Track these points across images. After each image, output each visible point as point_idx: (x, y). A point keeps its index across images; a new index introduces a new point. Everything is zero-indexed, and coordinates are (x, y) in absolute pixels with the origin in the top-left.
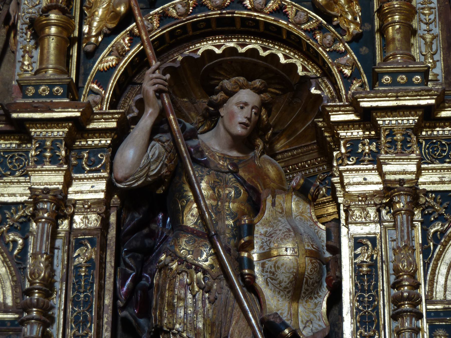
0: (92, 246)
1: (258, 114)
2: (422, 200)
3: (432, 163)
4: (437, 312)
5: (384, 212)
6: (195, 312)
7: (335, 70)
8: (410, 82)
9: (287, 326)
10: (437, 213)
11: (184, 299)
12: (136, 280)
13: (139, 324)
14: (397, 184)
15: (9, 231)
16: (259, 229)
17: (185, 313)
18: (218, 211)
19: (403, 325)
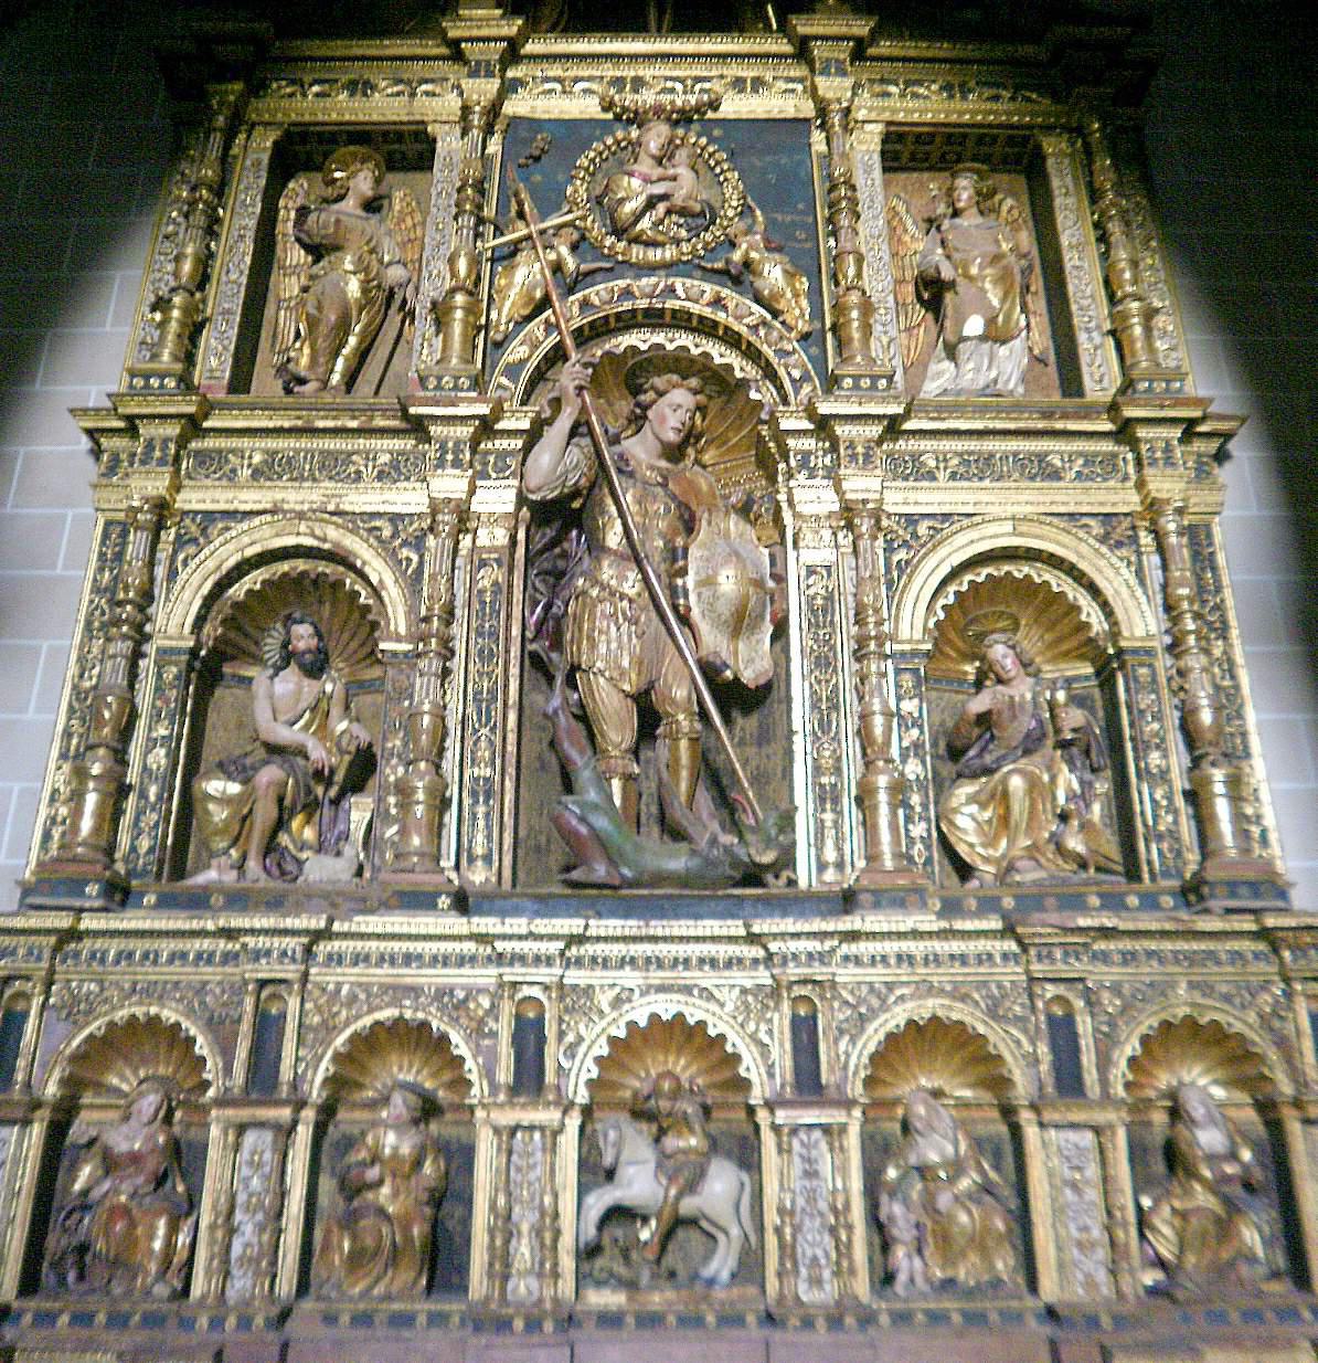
0: (500, 566)
1: (692, 418)
2: (885, 523)
4: (903, 654)
5: (840, 535)
6: (620, 647)
7: (782, 372)
8: (873, 387)
9: (728, 667)
11: (607, 633)
12: (548, 607)
13: (550, 659)
15: (401, 546)
16: (694, 552)
17: (608, 649)
18: (644, 529)
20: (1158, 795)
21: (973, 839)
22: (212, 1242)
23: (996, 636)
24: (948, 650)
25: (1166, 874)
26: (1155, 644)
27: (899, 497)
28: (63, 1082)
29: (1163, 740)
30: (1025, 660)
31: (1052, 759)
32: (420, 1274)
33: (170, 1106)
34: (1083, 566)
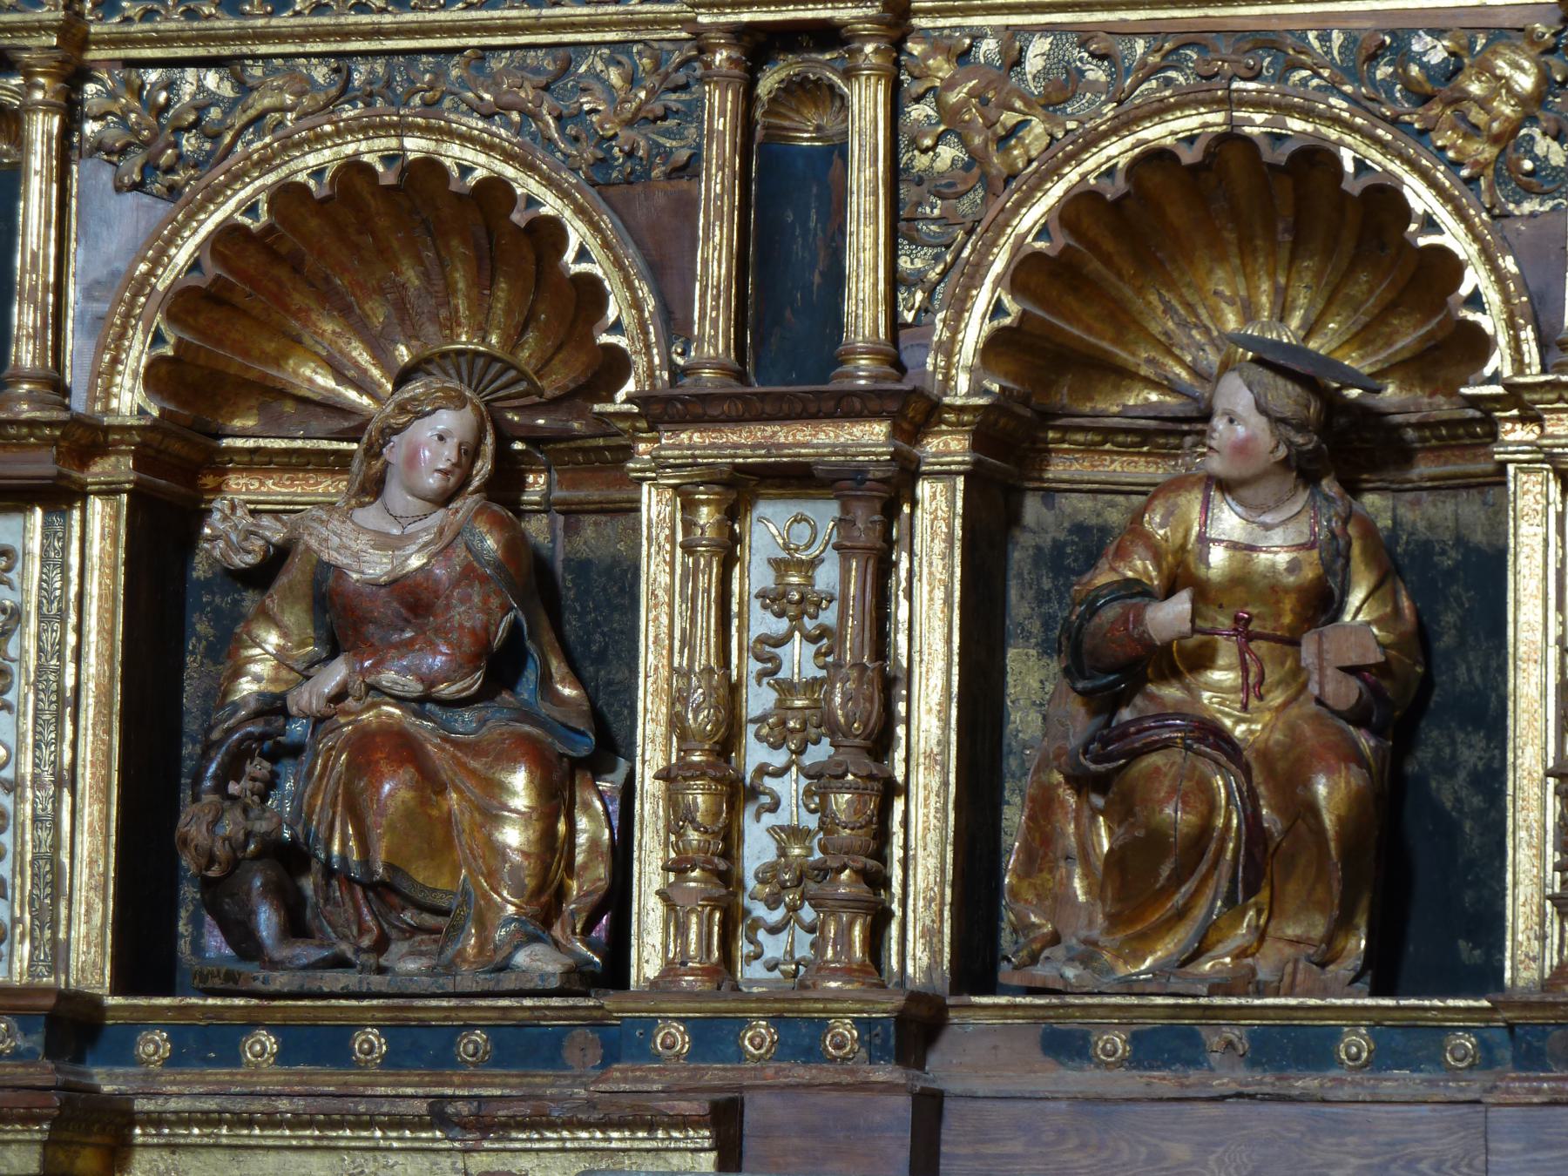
22: (678, 817)
28: (157, 377)
32: (1342, 924)
33: (503, 454)
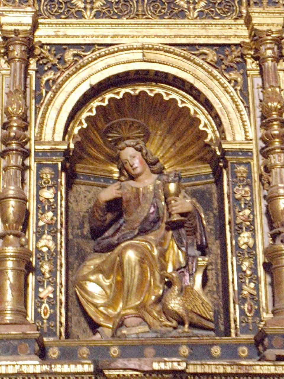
2: (37, 51)
3: (49, 18)
4: (45, 153)
10: (50, 63)
14: (12, 34)
19: (9, 161)
20: (245, 265)
21: (100, 301)
23: (128, 142)
24: (94, 152)
25: (245, 330)
26: (252, 146)
27: (51, 31)
29: (253, 223)
30: (151, 159)
31: (164, 238)
34: (198, 85)
